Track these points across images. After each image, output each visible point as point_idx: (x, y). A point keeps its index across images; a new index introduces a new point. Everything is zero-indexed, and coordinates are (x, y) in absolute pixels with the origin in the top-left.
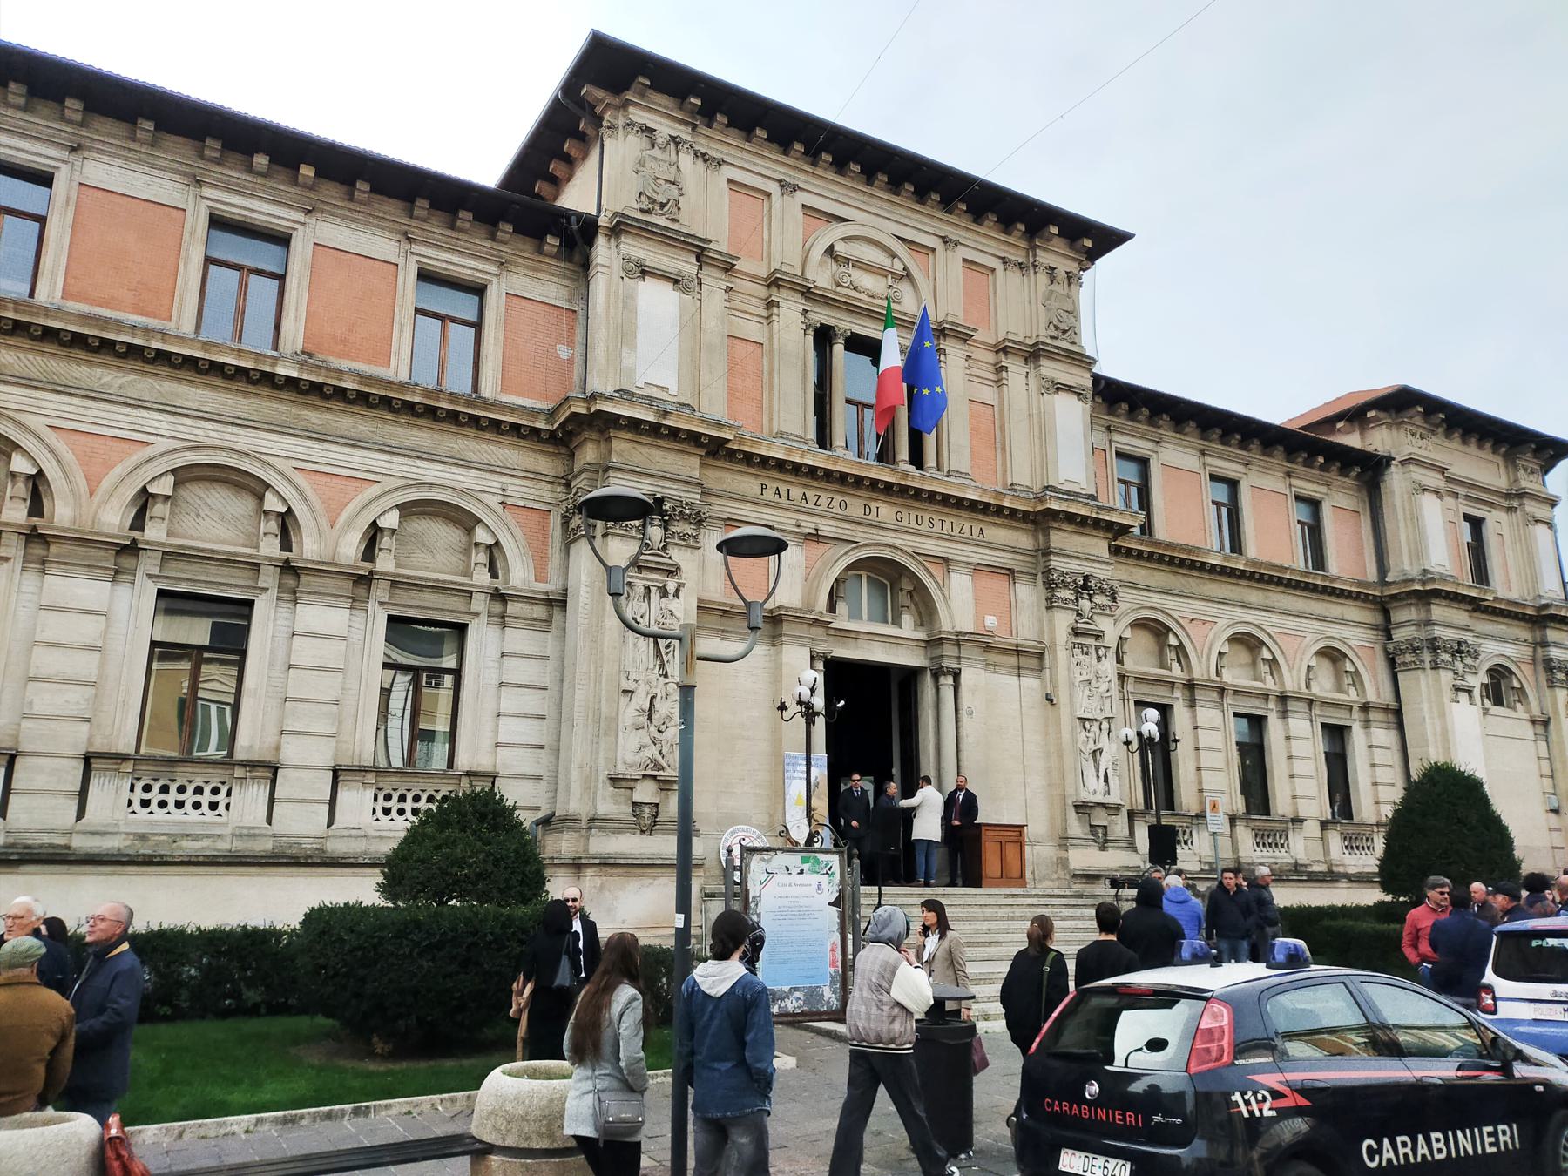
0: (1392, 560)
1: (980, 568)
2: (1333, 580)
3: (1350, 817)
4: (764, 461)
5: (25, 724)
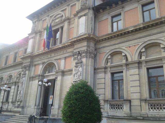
1: (65, 58)
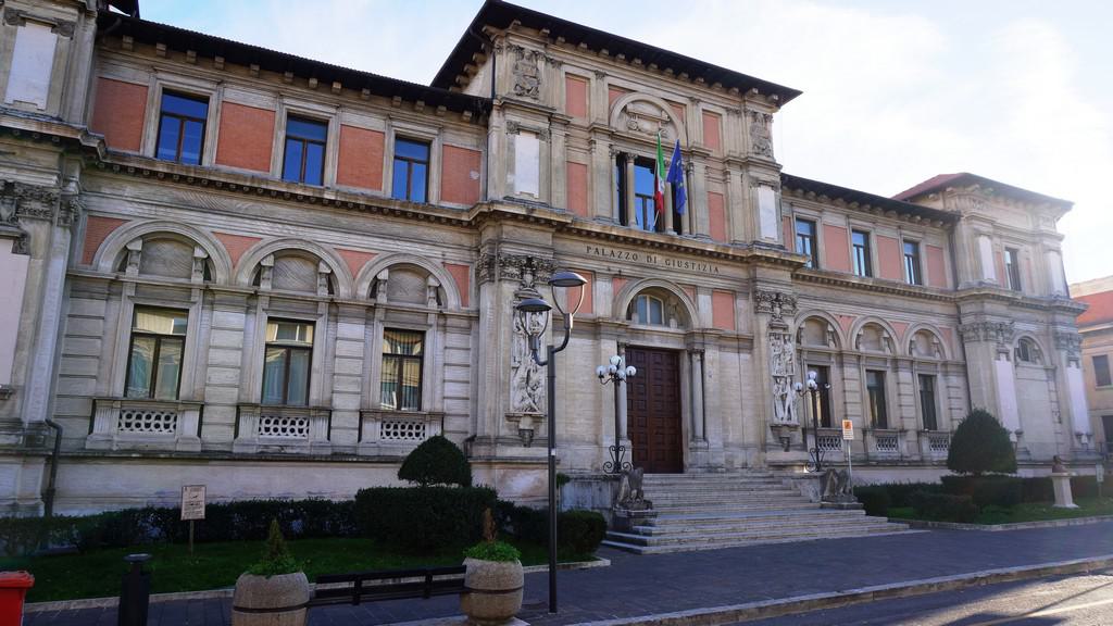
0: (961, 276)
2: (926, 290)
3: (936, 429)
4: (589, 233)
5: (207, 389)
